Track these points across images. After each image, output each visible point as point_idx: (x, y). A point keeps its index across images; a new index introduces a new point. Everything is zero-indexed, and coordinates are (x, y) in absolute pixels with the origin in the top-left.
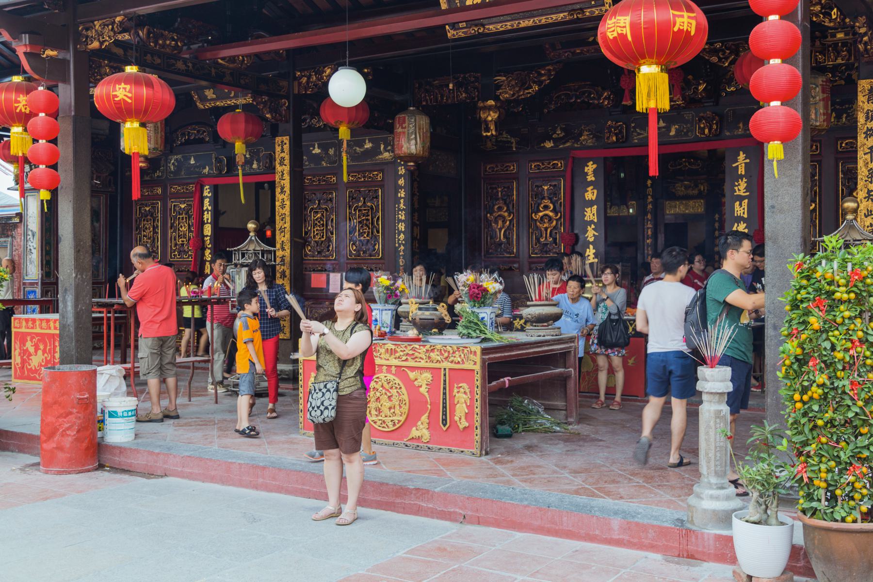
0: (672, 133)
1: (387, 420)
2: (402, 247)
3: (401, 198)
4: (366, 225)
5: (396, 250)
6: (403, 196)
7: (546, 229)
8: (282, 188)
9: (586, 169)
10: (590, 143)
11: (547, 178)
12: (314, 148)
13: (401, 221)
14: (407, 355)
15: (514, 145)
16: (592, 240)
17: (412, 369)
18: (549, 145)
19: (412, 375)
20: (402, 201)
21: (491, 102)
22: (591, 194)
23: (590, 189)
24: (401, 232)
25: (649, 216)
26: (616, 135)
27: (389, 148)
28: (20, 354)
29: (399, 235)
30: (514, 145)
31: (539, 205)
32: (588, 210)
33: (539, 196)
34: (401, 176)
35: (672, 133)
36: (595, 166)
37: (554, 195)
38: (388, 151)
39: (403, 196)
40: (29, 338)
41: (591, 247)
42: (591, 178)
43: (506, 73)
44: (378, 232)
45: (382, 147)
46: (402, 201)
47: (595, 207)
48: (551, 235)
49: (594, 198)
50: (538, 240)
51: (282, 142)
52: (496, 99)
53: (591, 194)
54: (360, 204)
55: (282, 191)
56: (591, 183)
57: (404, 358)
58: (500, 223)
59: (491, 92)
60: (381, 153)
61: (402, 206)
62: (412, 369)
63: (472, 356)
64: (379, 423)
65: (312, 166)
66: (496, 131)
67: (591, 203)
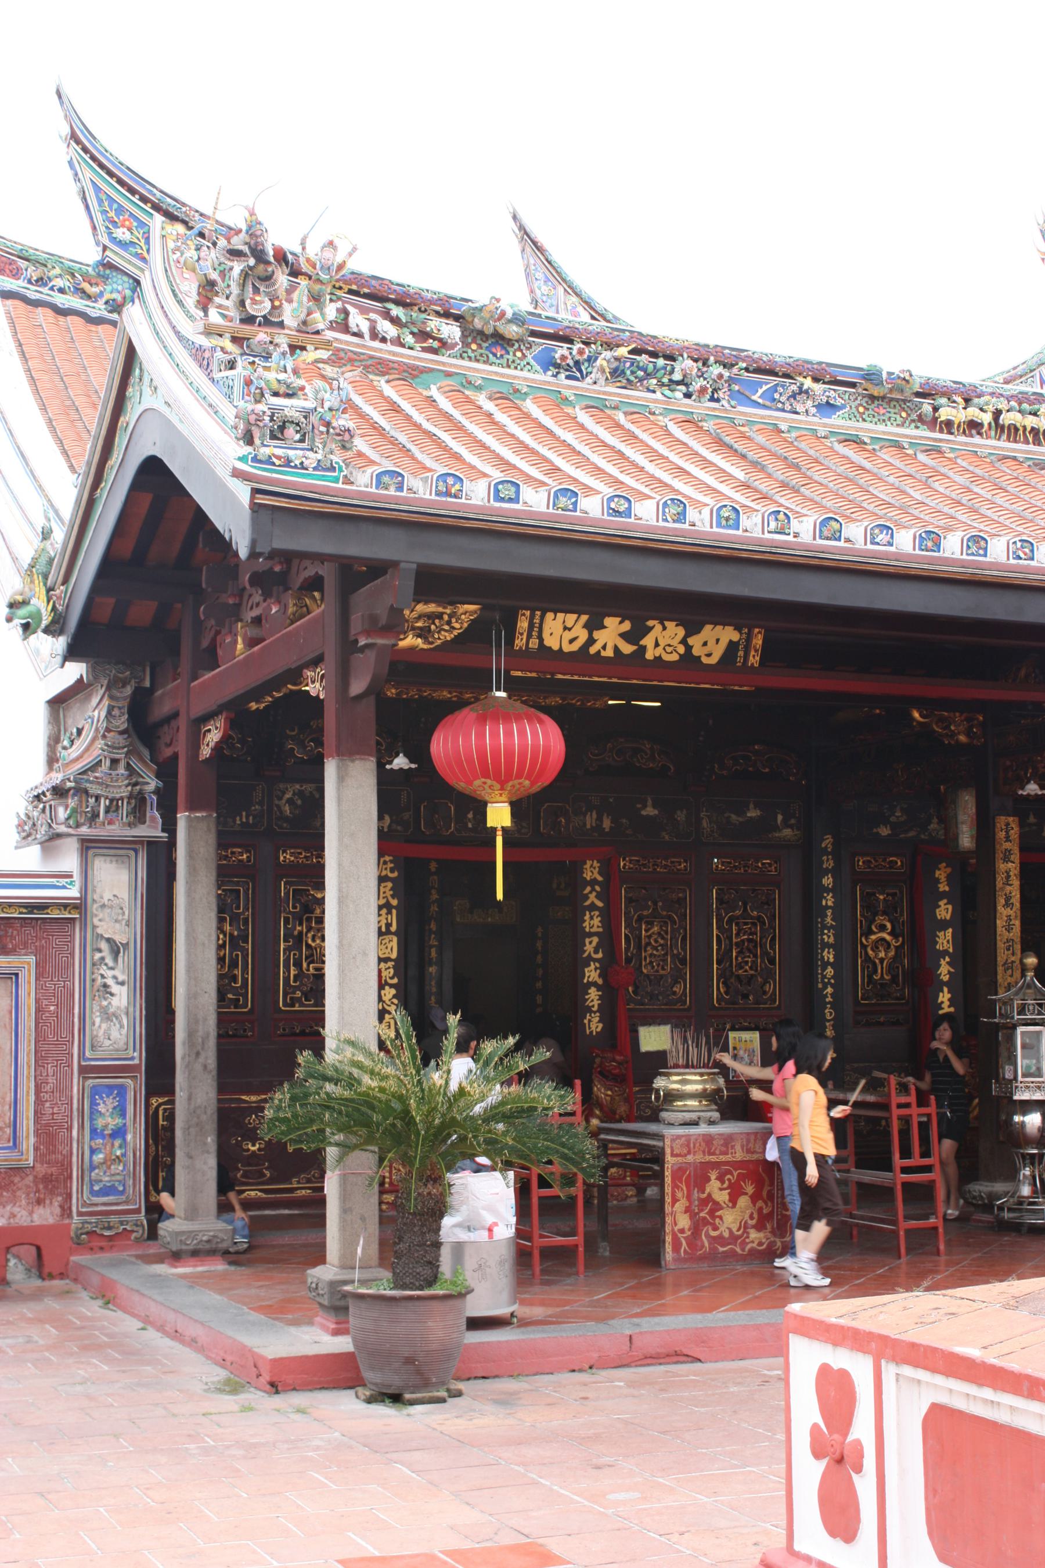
2: (829, 990)
3: (827, 907)
4: (750, 951)
6: (830, 903)
7: (882, 960)
8: (1008, 899)
9: (937, 873)
12: (645, 806)
16: (946, 978)
18: (885, 831)
20: (829, 913)
22: (944, 911)
23: (942, 903)
24: (828, 963)
25: (433, 926)
27: (793, 821)
28: (687, 1210)
29: (824, 969)
32: (941, 934)
36: (949, 870)
37: (890, 910)
38: (791, 827)
39: (830, 903)
40: (713, 1175)
41: (945, 989)
45: (780, 818)
46: (829, 913)
47: (950, 930)
48: (889, 972)
49: (948, 917)
50: (870, 977)
51: (1007, 824)
53: (944, 911)
54: (738, 913)
55: (1008, 904)
60: (777, 828)
67: (944, 925)
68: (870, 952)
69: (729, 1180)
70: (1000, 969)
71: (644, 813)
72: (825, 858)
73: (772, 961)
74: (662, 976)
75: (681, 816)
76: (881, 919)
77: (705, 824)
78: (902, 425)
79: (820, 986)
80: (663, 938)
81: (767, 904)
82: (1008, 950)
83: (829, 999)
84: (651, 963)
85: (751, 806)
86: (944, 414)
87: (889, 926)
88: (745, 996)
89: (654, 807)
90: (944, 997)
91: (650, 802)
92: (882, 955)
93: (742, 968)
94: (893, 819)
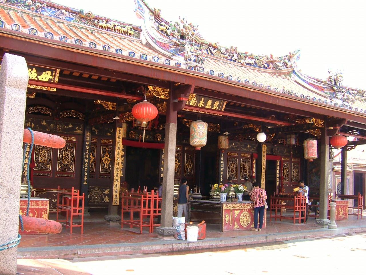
1: (245, 224)
2: (86, 169)
3: (87, 149)
8: (119, 147)
13: (87, 158)
15: (96, 132)
18: (109, 134)
20: (87, 150)
24: (86, 162)
27: (80, 129)
30: (96, 132)
33: (105, 152)
38: (80, 130)
39: (88, 148)
45: (77, 128)
46: (87, 150)
47: (123, 158)
50: (103, 167)
51: (120, 130)
55: (119, 148)
60: (76, 130)
61: (87, 152)
64: (244, 225)
69: (25, 212)
70: (115, 164)
71: (42, 124)
72: (87, 138)
73: (73, 161)
74: (44, 163)
75: (52, 125)
76: (107, 154)
77: (58, 127)
78: (89, 25)
79: (84, 167)
80: (45, 154)
81: (72, 147)
82: (118, 160)
84: (42, 159)
85: (70, 124)
86: (101, 24)
87: (108, 156)
88: (65, 169)
91: (44, 121)
92: (106, 162)
93: (65, 162)
94: (111, 132)
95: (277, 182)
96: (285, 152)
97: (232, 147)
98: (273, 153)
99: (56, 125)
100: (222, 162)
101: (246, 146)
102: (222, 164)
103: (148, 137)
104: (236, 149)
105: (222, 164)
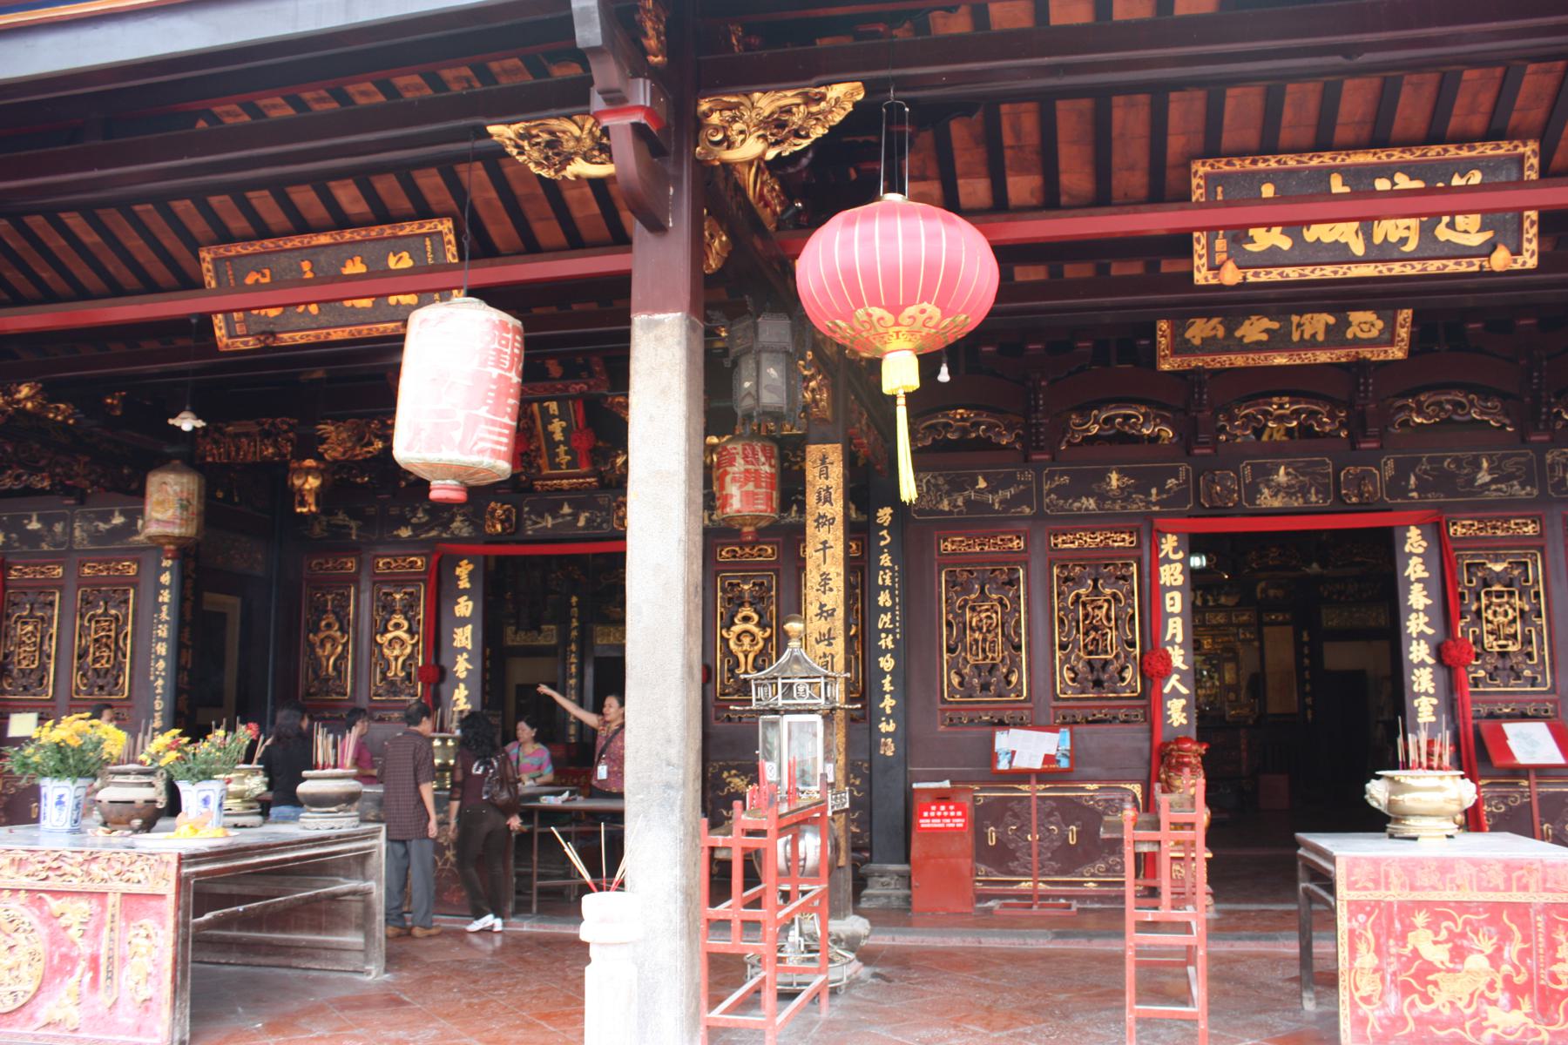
0: (581, 523)
4: (107, 646)
5: (150, 687)
7: (396, 658)
9: (458, 571)
10: (465, 532)
11: (400, 583)
13: (160, 639)
14: (50, 868)
17: (56, 894)
18: (405, 533)
19: (54, 905)
20: (165, 608)
21: (309, 463)
22: (464, 607)
25: (573, 647)
26: (502, 522)
30: (354, 532)
31: (388, 621)
32: (459, 631)
33: (389, 609)
34: (166, 569)
35: (581, 523)
36: (471, 567)
37: (409, 609)
42: (464, 584)
43: (336, 420)
44: (124, 656)
46: (165, 608)
52: (319, 457)
53: (464, 607)
54: (100, 611)
56: (464, 592)
57: (43, 875)
58: (328, 646)
59: (309, 445)
62: (56, 894)
63: (163, 869)
65: (25, 548)
66: (317, 504)
67: (463, 622)
68: (386, 651)
76: (398, 618)
77: (77, 533)
83: (159, 691)
89: (39, 520)
90: (461, 694)
94: (414, 520)
95: (1418, 695)
96: (1483, 477)
97: (967, 502)
98: (1339, 498)
99: (73, 522)
100: (884, 599)
101: (1088, 482)
102: (885, 610)
103: (588, 520)
104: (1005, 510)
105: (885, 610)
